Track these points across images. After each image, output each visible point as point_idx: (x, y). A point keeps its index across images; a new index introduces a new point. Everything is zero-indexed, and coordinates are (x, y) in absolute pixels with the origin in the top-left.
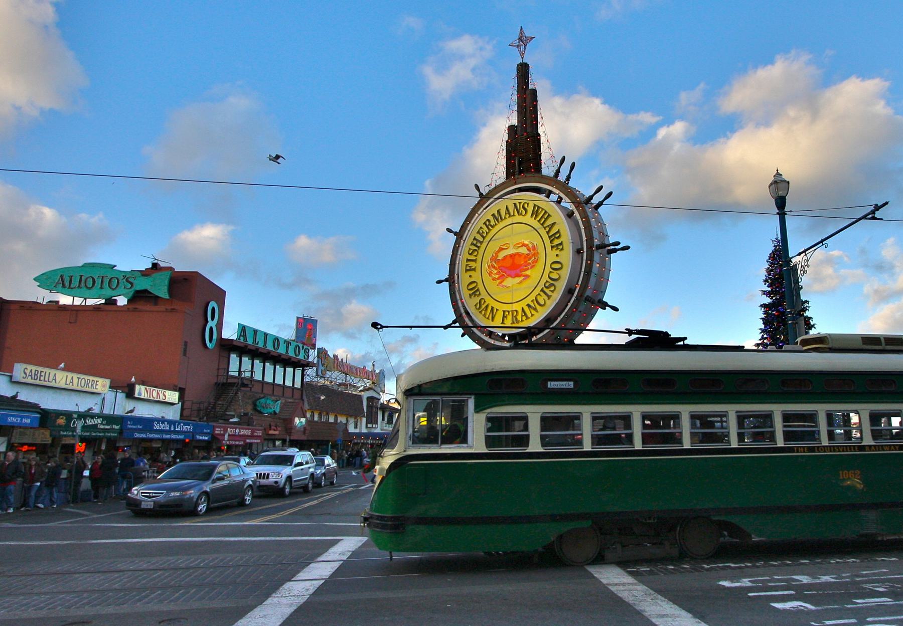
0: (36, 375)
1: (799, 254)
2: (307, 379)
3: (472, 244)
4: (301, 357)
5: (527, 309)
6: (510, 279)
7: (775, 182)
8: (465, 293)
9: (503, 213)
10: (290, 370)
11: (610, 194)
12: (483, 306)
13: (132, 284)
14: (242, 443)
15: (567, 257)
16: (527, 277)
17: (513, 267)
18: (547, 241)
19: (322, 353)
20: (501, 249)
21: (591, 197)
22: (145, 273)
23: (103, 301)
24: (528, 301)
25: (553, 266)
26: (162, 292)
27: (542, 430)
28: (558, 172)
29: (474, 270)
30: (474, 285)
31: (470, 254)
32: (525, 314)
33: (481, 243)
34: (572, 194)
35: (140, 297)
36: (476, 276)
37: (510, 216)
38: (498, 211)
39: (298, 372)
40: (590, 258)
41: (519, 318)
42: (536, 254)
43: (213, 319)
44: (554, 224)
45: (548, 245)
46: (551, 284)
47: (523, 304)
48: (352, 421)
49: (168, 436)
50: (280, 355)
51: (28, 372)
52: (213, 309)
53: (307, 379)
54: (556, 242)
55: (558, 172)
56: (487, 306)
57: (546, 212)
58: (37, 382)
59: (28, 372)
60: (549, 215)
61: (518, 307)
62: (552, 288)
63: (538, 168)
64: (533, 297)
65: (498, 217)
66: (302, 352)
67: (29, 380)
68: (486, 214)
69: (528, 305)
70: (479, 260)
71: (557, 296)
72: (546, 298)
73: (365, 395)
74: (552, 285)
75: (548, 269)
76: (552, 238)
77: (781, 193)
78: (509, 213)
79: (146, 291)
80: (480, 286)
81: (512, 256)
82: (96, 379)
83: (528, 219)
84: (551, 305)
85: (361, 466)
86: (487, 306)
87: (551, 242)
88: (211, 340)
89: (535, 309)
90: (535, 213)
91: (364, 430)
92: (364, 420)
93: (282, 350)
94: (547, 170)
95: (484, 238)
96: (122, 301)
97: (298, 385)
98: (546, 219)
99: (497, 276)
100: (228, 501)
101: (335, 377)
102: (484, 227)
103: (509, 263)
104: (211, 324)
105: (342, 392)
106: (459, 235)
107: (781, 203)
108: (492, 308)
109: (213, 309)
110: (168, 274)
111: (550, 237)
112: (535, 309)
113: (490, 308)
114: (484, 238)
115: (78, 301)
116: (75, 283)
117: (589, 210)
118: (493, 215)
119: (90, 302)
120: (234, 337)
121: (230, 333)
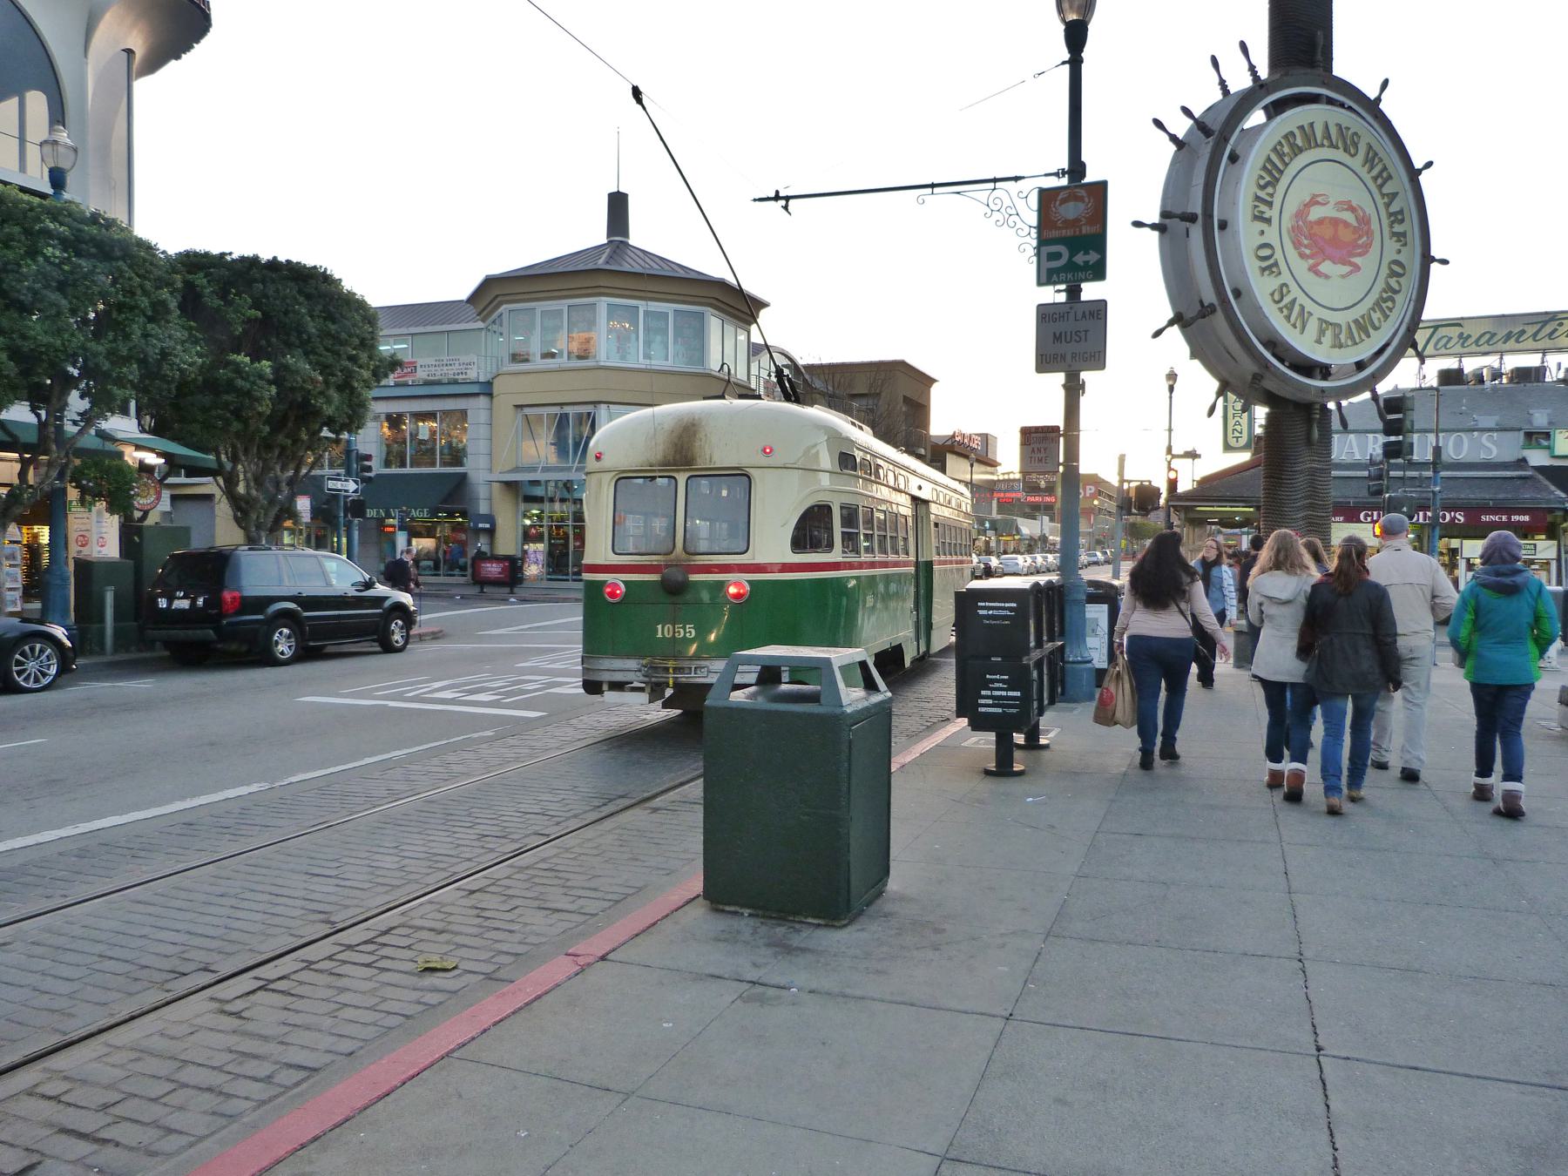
3: (1264, 168)
6: (1328, 263)
12: (1286, 300)
16: (1357, 268)
18: (1385, 222)
20: (1314, 201)
29: (1268, 221)
31: (1263, 188)
32: (1351, 337)
33: (1281, 172)
41: (1343, 337)
42: (1369, 233)
56: (1294, 300)
57: (1385, 168)
60: (1390, 177)
62: (1390, 304)
69: (1356, 321)
70: (1277, 205)
75: (1385, 271)
78: (1329, 137)
80: (1278, 255)
81: (1335, 222)
83: (1357, 162)
86: (1294, 300)
99: (1308, 252)
108: (1302, 308)
111: (1391, 215)
113: (1297, 309)
114: (1286, 165)
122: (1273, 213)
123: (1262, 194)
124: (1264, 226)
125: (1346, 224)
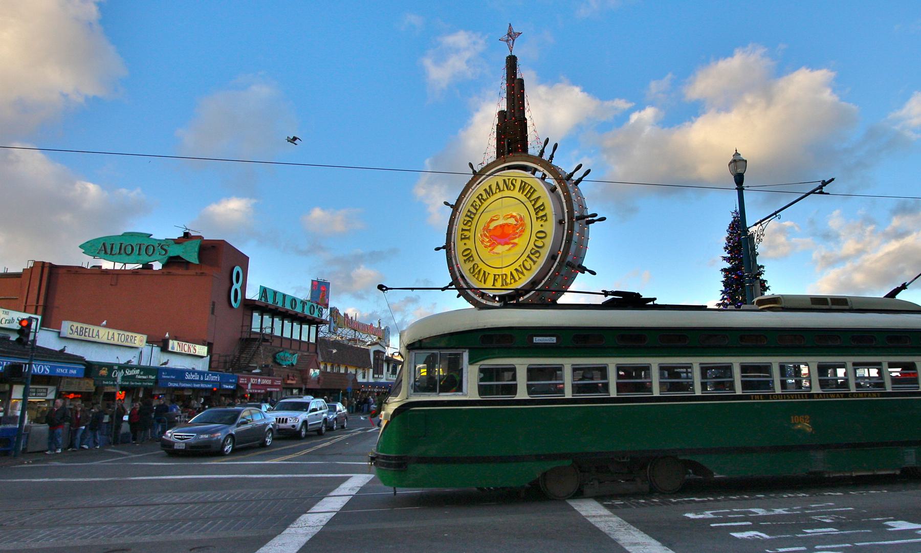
0: (82, 331)
1: (756, 225)
2: (321, 335)
3: (467, 215)
4: (315, 315)
5: (515, 273)
6: (500, 246)
7: (734, 161)
8: (460, 259)
9: (494, 188)
10: (305, 327)
11: (588, 171)
12: (477, 271)
13: (166, 251)
14: (263, 391)
15: (550, 227)
16: (515, 244)
17: (502, 236)
19: (334, 312)
20: (492, 220)
21: (572, 174)
22: (178, 242)
23: (141, 266)
24: (516, 266)
25: (540, 235)
26: (193, 258)
27: (528, 380)
28: (542, 152)
29: (468, 238)
30: (468, 252)
33: (475, 214)
34: (555, 171)
35: (173, 262)
36: (470, 244)
37: (500, 191)
38: (490, 187)
39: (313, 329)
40: (571, 228)
41: (508, 281)
42: (523, 225)
43: (237, 282)
44: (539, 198)
45: (534, 217)
46: (537, 250)
47: (512, 268)
48: (360, 372)
49: (198, 386)
50: (297, 314)
51: (74, 329)
52: (238, 273)
53: (321, 335)
54: (541, 214)
55: (542, 152)
56: (480, 271)
58: (83, 337)
59: (74, 329)
61: (506, 271)
62: (537, 255)
63: (525, 149)
64: (520, 262)
65: (489, 192)
66: (316, 310)
67: (75, 336)
68: (479, 189)
69: (516, 270)
71: (541, 261)
72: (532, 263)
73: (372, 349)
74: (538, 252)
75: (534, 238)
76: (537, 211)
77: (739, 171)
79: (178, 257)
80: (474, 253)
81: (502, 226)
82: (134, 335)
83: (516, 193)
84: (536, 269)
85: (369, 411)
86: (480, 271)
87: (536, 214)
88: (236, 300)
89: (522, 273)
90: (522, 189)
91: (371, 380)
92: (371, 370)
93: (298, 309)
94: (533, 150)
95: (477, 210)
96: (157, 266)
97: (313, 340)
98: (532, 194)
100: (251, 443)
101: (346, 333)
102: (477, 200)
103: (499, 232)
104: (237, 286)
105: (352, 347)
106: (455, 208)
107: (739, 179)
109: (238, 273)
110: (198, 242)
112: (522, 273)
114: (477, 210)
115: (118, 266)
116: (116, 249)
117: (570, 186)
118: (485, 190)
119: (129, 267)
120: (257, 298)
121: (252, 294)
122: (471, 234)
123: (466, 227)
124: (466, 241)
125: (508, 225)
